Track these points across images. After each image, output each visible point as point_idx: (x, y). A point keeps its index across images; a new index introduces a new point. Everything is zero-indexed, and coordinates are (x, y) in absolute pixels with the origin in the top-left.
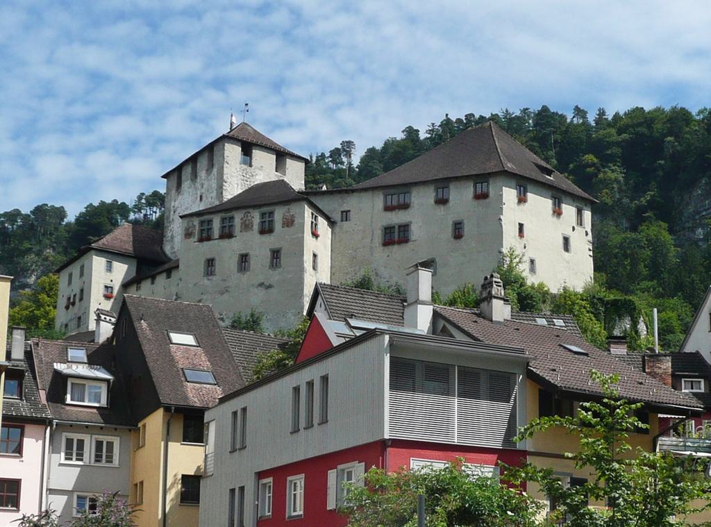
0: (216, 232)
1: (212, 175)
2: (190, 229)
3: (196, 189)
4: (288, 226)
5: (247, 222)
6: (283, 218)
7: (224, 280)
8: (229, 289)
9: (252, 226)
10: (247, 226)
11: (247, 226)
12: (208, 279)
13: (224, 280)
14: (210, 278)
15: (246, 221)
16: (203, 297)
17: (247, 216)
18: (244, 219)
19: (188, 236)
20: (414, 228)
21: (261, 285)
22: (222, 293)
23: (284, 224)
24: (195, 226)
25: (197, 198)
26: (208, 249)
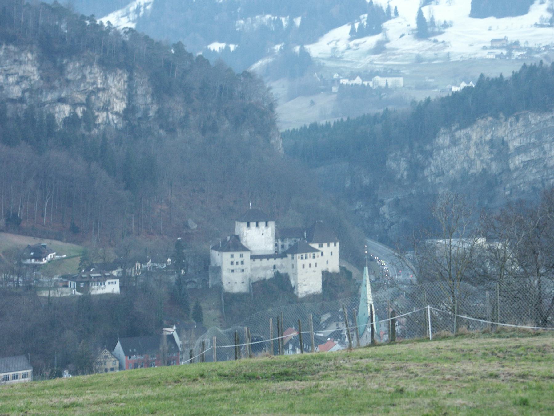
0: (304, 258)
11: (310, 257)
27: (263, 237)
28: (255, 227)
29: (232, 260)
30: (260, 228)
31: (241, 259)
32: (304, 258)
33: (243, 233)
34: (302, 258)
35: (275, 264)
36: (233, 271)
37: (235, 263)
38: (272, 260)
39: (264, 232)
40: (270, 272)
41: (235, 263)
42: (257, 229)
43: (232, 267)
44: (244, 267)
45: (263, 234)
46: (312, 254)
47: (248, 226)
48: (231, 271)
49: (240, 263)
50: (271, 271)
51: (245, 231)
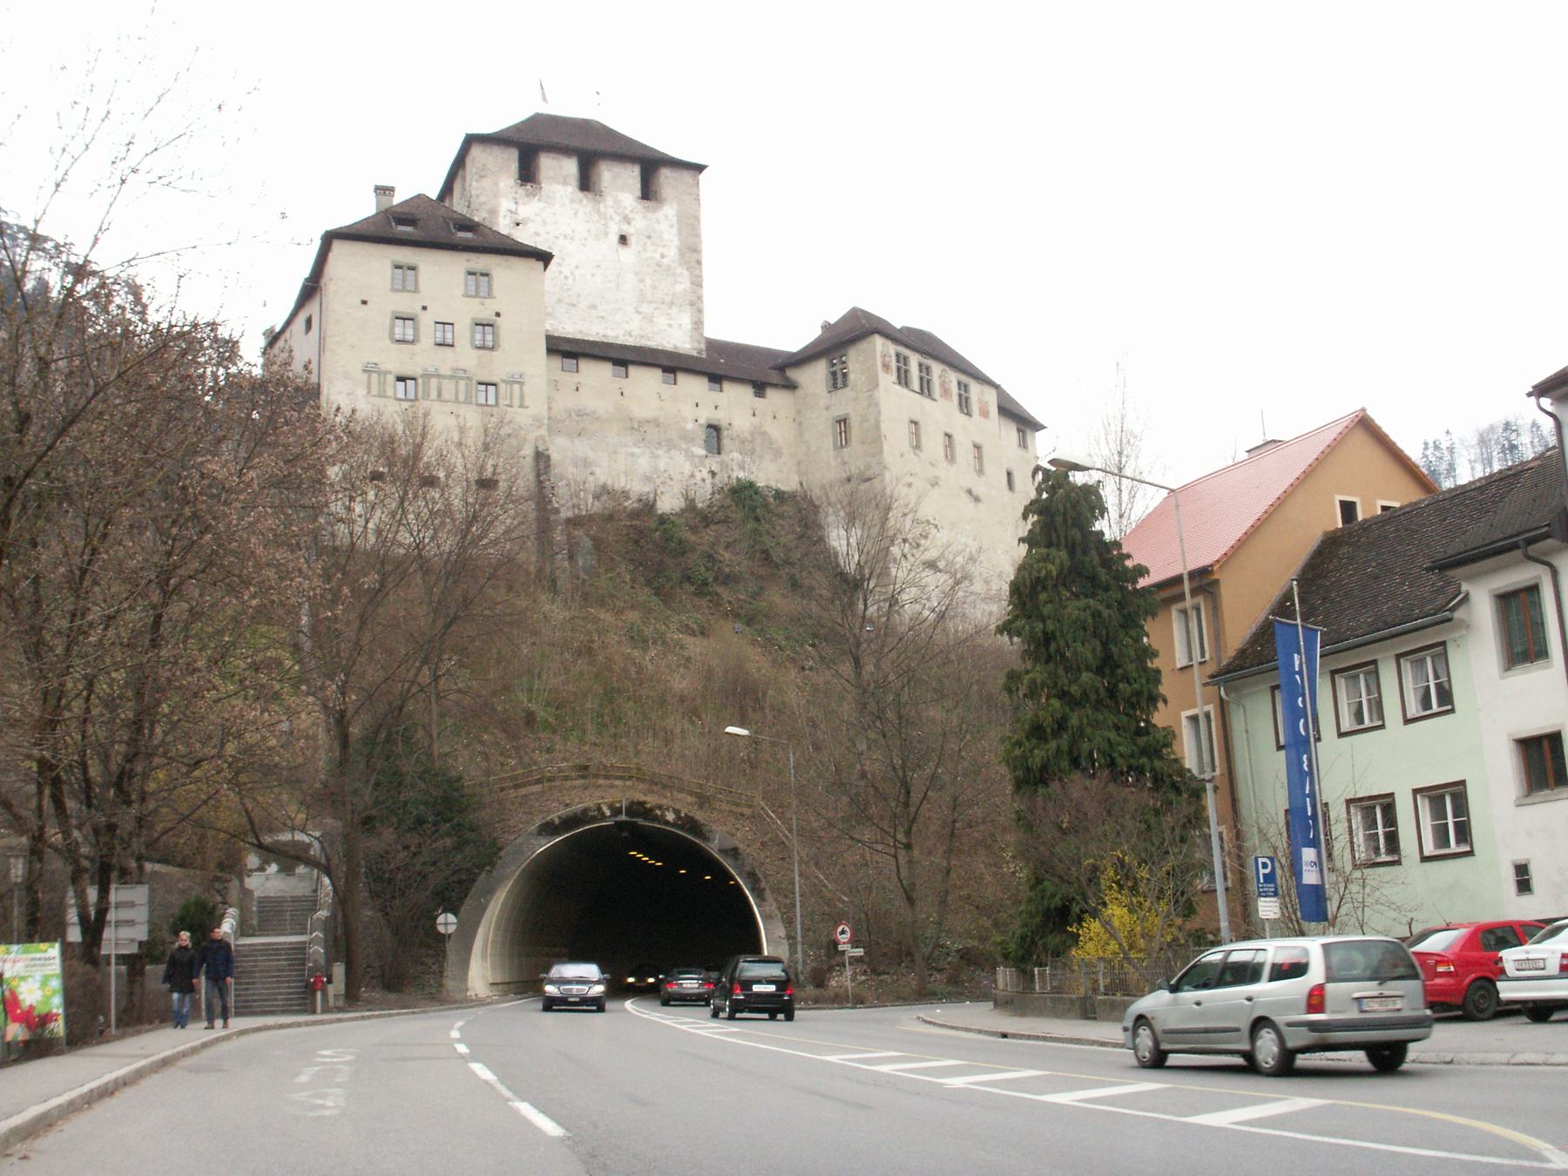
1: (660, 215)
21: (970, 492)
25: (606, 234)
27: (626, 254)
28: (572, 189)
29: (406, 304)
30: (609, 201)
33: (493, 212)
35: (721, 417)
38: (693, 387)
39: (627, 229)
40: (687, 468)
42: (585, 202)
44: (498, 366)
45: (623, 239)
47: (527, 174)
48: (391, 379)
49: (462, 333)
50: (691, 456)
51: (505, 204)
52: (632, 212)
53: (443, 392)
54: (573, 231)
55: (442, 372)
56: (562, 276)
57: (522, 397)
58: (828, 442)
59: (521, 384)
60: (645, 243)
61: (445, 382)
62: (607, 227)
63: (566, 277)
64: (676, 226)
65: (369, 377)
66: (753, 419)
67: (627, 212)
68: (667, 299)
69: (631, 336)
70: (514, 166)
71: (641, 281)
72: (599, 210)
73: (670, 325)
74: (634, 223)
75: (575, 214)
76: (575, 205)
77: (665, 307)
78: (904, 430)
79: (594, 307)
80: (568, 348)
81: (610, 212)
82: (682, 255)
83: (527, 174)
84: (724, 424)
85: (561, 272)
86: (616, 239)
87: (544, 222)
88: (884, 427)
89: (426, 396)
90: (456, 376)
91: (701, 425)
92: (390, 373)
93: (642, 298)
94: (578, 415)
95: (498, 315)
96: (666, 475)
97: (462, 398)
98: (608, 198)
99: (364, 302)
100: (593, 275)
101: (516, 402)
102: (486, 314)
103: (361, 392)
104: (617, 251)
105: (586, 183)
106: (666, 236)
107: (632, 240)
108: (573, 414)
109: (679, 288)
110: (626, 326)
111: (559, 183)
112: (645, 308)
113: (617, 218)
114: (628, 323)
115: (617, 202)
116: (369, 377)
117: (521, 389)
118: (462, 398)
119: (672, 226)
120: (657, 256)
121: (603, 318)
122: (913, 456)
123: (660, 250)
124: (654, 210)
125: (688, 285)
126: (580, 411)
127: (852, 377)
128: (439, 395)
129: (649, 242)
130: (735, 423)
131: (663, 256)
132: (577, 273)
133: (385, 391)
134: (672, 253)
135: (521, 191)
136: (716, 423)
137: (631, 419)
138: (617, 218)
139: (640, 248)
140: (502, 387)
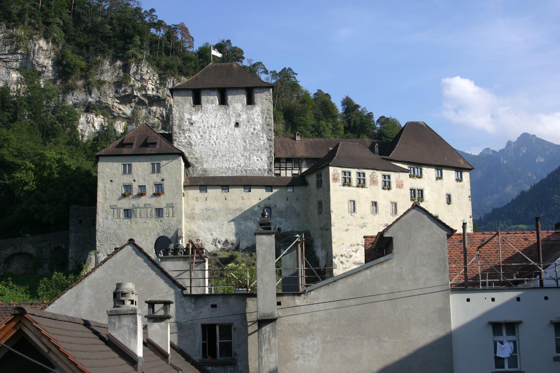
0: (354, 182)
2: (336, 176)
3: (228, 115)
4: (399, 188)
5: (374, 179)
6: (396, 182)
7: (362, 218)
8: (366, 225)
9: (378, 182)
10: (374, 182)
11: (374, 182)
12: (351, 215)
13: (362, 218)
14: (352, 214)
15: (373, 178)
16: (349, 227)
17: (374, 175)
18: (372, 176)
19: (335, 180)
20: (425, 193)
22: (362, 227)
23: (397, 185)
24: (339, 174)
26: (353, 192)
29: (127, 180)
31: (156, 178)
32: (354, 182)
34: (347, 183)
36: (128, 213)
37: (136, 191)
41: (136, 191)
42: (221, 111)
43: (126, 203)
44: (162, 202)
45: (237, 125)
46: (379, 175)
47: (197, 102)
48: (122, 211)
49: (150, 190)
51: (187, 116)
52: (241, 111)
53: (142, 214)
54: (215, 123)
55: (141, 206)
56: (211, 144)
57: (173, 213)
58: (316, 212)
59: (173, 207)
60: (247, 124)
61: (142, 210)
62: (230, 120)
63: (212, 144)
64: (261, 115)
65: (114, 211)
66: (287, 202)
67: (239, 112)
68: (256, 148)
69: (240, 167)
70: (190, 99)
71: (245, 142)
72: (226, 112)
73: (258, 160)
74: (242, 117)
75: (216, 116)
76: (215, 112)
77: (256, 152)
78: (346, 207)
79: (225, 156)
80: (202, 183)
81: (231, 112)
82: (263, 127)
83: (197, 102)
84: (272, 206)
85: (210, 143)
86: (234, 124)
87: (203, 121)
88: (333, 207)
89: (135, 216)
90: (146, 206)
91: (261, 208)
92: (122, 208)
93: (245, 149)
94: (207, 211)
95: (163, 180)
96: (245, 232)
97: (149, 216)
98: (231, 107)
99: (111, 181)
100: (224, 142)
101: (171, 215)
102: (159, 181)
103: (110, 217)
104: (234, 130)
105: (223, 102)
106: (256, 120)
107: (241, 124)
108: (204, 210)
109: (262, 142)
110: (238, 162)
111: (209, 103)
112: (247, 154)
113: (234, 115)
114: (239, 161)
115: (234, 108)
116: (114, 211)
117: (172, 209)
118: (149, 216)
119: (258, 115)
120: (252, 130)
121: (228, 160)
122: (350, 216)
123: (253, 127)
124: (252, 109)
125: (266, 140)
126: (207, 209)
127: (323, 183)
128: (140, 215)
129: (248, 124)
130: (278, 205)
131: (254, 129)
132: (217, 143)
133: (119, 216)
134: (258, 127)
135: (193, 109)
136: (268, 206)
137: (230, 210)
138: (234, 115)
139: (244, 127)
140: (165, 210)
